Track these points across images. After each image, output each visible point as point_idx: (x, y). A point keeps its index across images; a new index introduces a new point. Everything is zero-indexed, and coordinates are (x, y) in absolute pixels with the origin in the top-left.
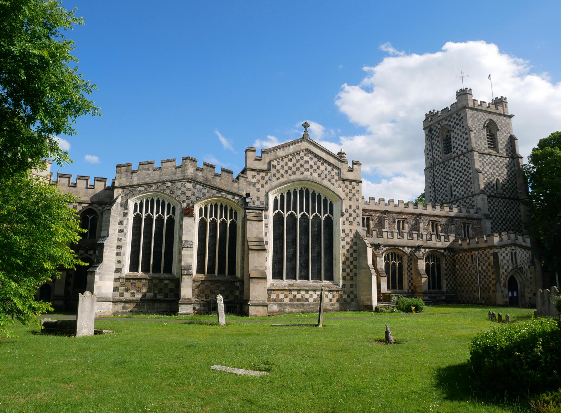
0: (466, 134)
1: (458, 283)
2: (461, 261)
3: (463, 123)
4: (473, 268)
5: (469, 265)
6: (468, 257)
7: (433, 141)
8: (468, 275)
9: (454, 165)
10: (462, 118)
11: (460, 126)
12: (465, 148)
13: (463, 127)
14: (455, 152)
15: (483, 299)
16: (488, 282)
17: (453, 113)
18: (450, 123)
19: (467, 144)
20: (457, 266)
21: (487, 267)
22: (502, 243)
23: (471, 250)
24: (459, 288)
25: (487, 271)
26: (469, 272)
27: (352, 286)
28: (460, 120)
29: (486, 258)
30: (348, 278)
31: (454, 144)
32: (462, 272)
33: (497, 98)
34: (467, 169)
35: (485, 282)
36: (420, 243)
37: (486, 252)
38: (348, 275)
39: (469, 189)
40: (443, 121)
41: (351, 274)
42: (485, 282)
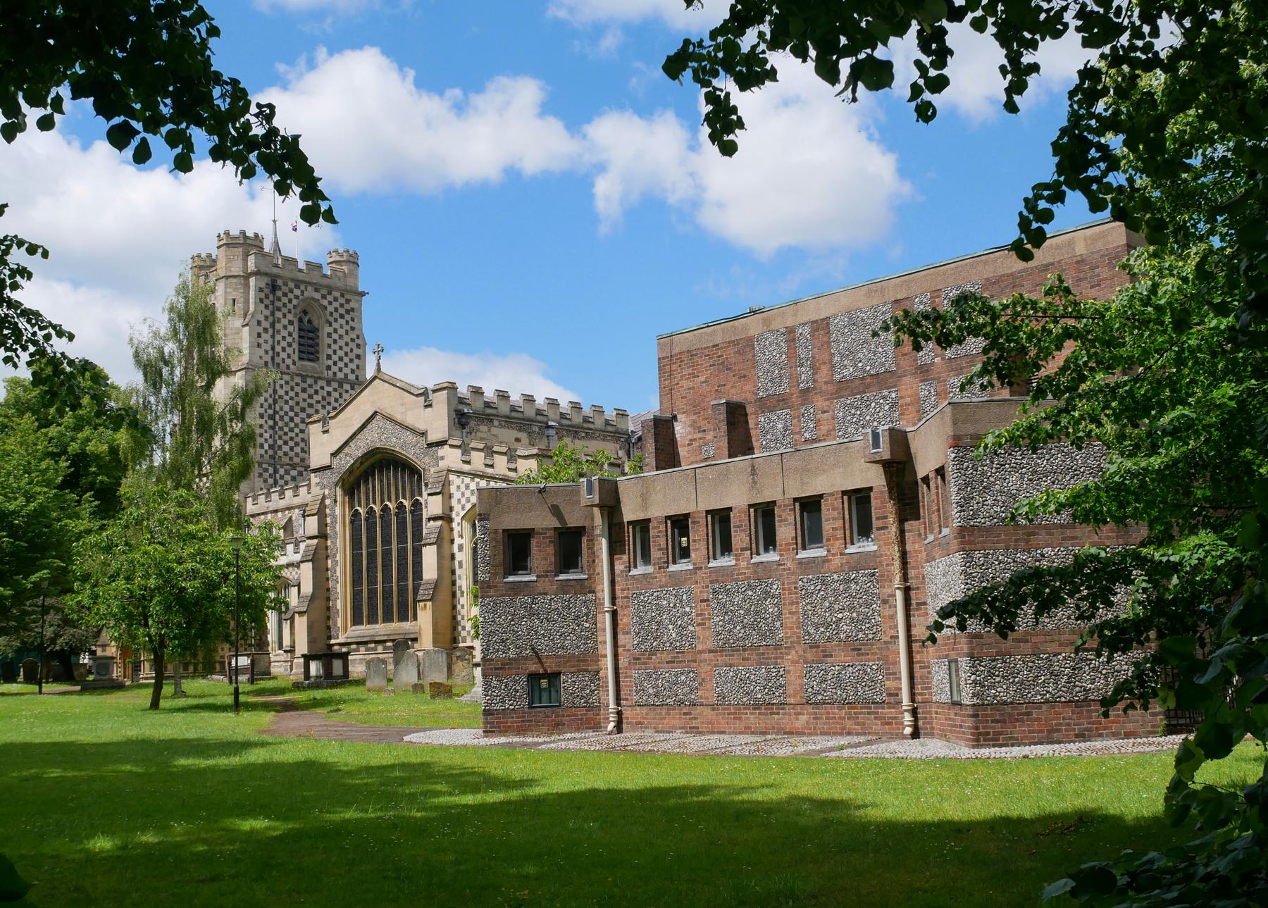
3: (353, 320)
9: (329, 394)
17: (337, 289)
19: (358, 367)
28: (348, 312)
40: (309, 288)
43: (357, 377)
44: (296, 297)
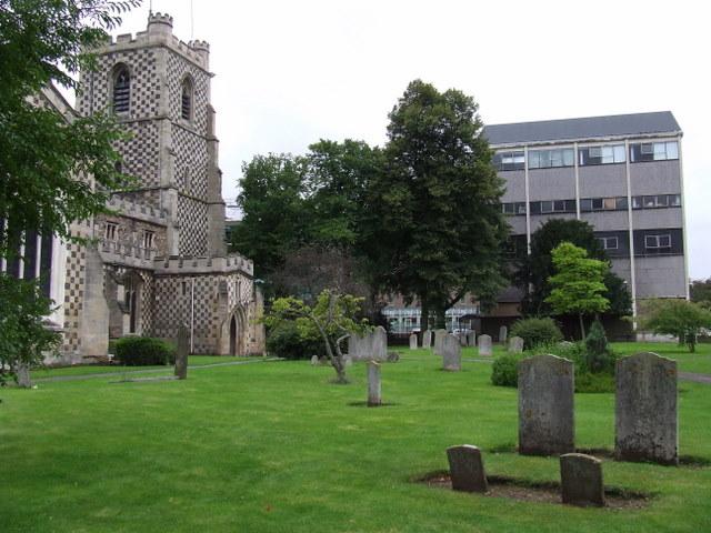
0: (158, 88)
1: (157, 323)
2: (165, 289)
3: (154, 68)
4: (185, 302)
5: (178, 298)
6: (178, 285)
7: (96, 83)
8: (175, 311)
10: (154, 60)
11: (149, 72)
12: (153, 109)
13: (154, 75)
14: (133, 112)
15: (196, 346)
16: (206, 322)
17: (141, 49)
18: (132, 62)
19: (157, 105)
20: (158, 298)
21: (207, 301)
22: (230, 269)
23: (184, 275)
24: (158, 331)
25: (207, 307)
26: (178, 307)
27: (76, 325)
28: (150, 63)
29: (207, 288)
30: (72, 311)
31: (135, 99)
32: (164, 307)
33: (197, 41)
34: (153, 145)
35: (202, 322)
36: (117, 259)
37: (207, 279)
38: (72, 307)
39: (152, 176)
41: (76, 305)
42: (202, 322)
43: (156, 114)
44: (110, 65)
